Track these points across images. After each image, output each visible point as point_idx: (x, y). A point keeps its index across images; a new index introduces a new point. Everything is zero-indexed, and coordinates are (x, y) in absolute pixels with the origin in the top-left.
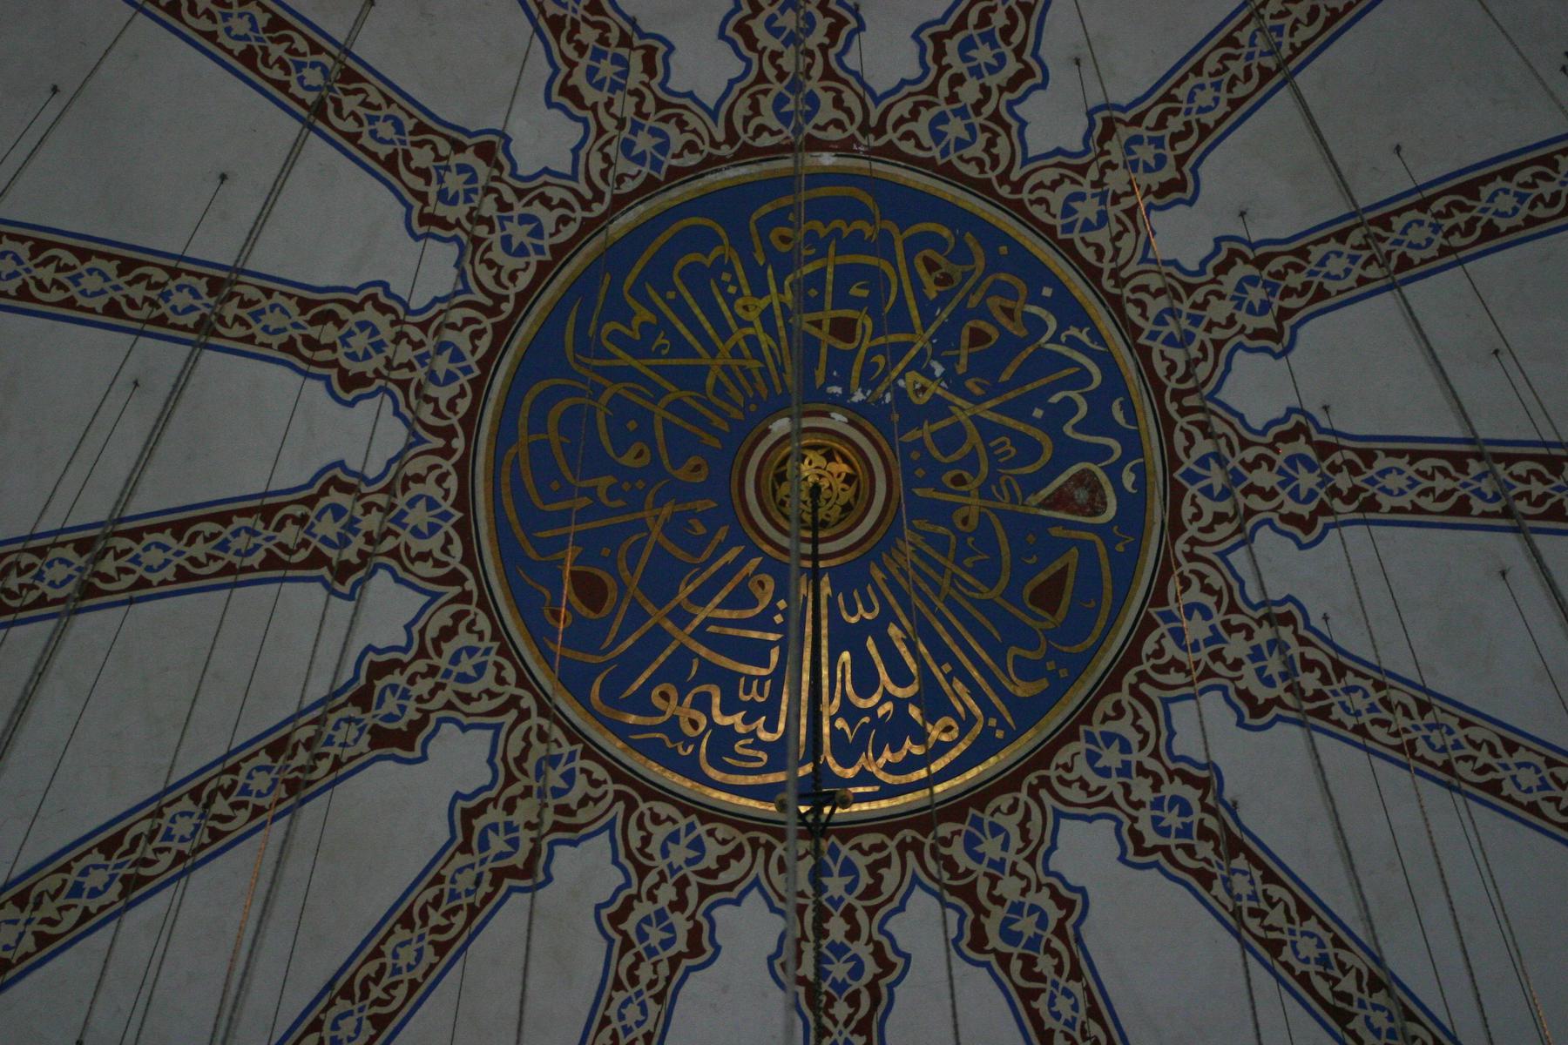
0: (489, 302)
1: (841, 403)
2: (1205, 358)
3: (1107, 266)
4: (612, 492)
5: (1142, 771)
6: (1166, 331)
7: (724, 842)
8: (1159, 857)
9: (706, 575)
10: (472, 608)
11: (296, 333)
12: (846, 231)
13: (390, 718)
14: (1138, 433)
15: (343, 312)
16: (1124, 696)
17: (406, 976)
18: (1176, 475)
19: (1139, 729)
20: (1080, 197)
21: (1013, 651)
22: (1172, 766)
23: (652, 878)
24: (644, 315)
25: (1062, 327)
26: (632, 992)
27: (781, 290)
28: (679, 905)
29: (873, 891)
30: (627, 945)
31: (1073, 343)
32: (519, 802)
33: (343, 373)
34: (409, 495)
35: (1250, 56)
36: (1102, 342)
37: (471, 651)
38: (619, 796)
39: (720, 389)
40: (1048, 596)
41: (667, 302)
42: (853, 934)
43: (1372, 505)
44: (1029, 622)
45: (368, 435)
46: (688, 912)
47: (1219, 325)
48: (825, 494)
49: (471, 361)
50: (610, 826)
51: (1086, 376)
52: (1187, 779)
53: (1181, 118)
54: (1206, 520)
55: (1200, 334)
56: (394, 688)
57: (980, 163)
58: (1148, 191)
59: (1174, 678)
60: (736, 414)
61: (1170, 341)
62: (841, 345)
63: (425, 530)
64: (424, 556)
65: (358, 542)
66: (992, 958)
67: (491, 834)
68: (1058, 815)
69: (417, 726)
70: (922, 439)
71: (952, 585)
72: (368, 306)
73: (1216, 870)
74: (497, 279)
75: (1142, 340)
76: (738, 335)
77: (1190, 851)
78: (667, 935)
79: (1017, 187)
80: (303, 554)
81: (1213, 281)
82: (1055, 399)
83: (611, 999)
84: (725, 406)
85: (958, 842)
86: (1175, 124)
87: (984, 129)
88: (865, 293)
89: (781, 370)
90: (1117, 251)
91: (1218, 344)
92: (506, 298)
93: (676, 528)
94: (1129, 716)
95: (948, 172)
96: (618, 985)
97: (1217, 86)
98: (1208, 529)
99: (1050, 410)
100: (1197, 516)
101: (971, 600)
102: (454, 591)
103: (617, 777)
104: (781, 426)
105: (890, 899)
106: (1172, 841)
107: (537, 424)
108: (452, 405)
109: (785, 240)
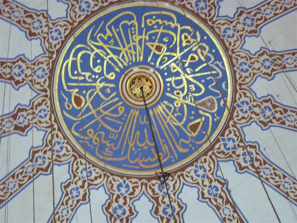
0: (71, 22)
1: (154, 67)
2: (250, 76)
3: (231, 48)
4: (90, 77)
5: (208, 177)
6: (241, 68)
7: (97, 173)
8: (208, 200)
9: (108, 104)
10: (47, 99)
11: (22, 19)
12: (167, 24)
13: (20, 123)
14: (227, 92)
15: (34, 16)
16: (208, 158)
17: (10, 191)
18: (235, 105)
19: (210, 167)
20: (229, 29)
21: (182, 140)
22: (216, 178)
23: (77, 178)
24: (109, 33)
25: (215, 60)
26: (66, 207)
27: (146, 35)
28: (82, 187)
29: (132, 194)
30: (67, 194)
31: (217, 65)
32: (47, 152)
33: (30, 32)
34: (39, 67)
35: (283, 4)
36: (224, 67)
37: (45, 110)
38: (73, 155)
39: (123, 57)
40: (194, 128)
41: (117, 32)
42: (125, 203)
43: (283, 123)
44: (187, 133)
45: (34, 49)
46: (85, 189)
47: (256, 69)
48: (144, 89)
49: (63, 36)
50: (69, 163)
51: (218, 74)
52: (219, 182)
53: (261, 15)
54: (240, 117)
55: (250, 70)
56: (23, 116)
57: (206, 15)
58: (247, 31)
59: (221, 155)
60: (126, 64)
61: (242, 70)
62: (157, 53)
63: (40, 77)
64: (38, 83)
65: (23, 76)
66: (159, 217)
67: (39, 159)
68: (184, 184)
69: (26, 127)
70: (171, 81)
71: (170, 119)
72: (41, 16)
73: (221, 207)
74: (75, 16)
75: (235, 68)
76: (132, 44)
77: (216, 201)
78: (77, 194)
79: (214, 23)
80: (8, 76)
81: (257, 58)
82: (208, 78)
83: (60, 207)
84: (123, 62)
85: (157, 186)
86: (259, 16)
87: (209, 6)
88: (167, 41)
89: (140, 55)
90: (235, 45)
91: (254, 74)
92: (76, 22)
93: (103, 90)
94: (208, 162)
95: (197, 15)
96: (63, 204)
97: (272, 9)
98: (240, 120)
99: (206, 80)
100: (238, 116)
101: (174, 125)
102: (44, 94)
103: (74, 150)
104: (136, 69)
105: (136, 196)
106: (212, 197)
107: (75, 55)
108: (55, 46)
109: (151, 23)
